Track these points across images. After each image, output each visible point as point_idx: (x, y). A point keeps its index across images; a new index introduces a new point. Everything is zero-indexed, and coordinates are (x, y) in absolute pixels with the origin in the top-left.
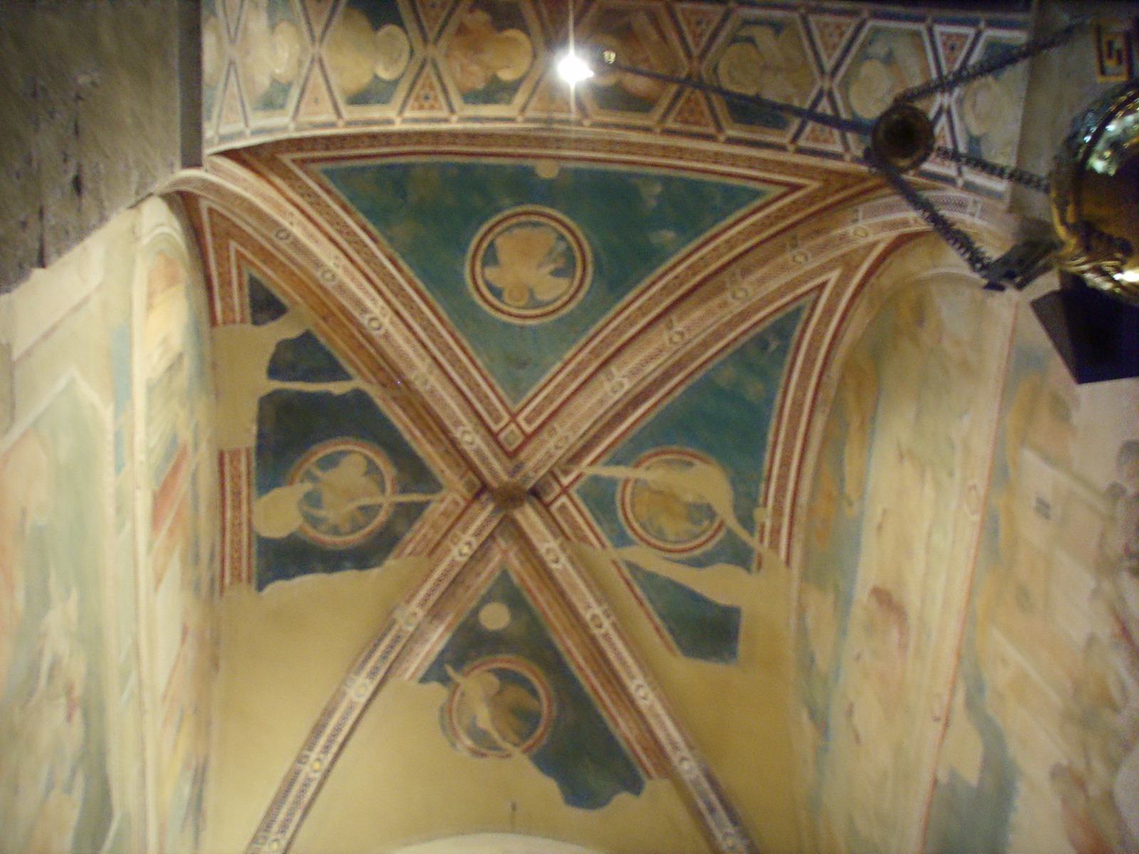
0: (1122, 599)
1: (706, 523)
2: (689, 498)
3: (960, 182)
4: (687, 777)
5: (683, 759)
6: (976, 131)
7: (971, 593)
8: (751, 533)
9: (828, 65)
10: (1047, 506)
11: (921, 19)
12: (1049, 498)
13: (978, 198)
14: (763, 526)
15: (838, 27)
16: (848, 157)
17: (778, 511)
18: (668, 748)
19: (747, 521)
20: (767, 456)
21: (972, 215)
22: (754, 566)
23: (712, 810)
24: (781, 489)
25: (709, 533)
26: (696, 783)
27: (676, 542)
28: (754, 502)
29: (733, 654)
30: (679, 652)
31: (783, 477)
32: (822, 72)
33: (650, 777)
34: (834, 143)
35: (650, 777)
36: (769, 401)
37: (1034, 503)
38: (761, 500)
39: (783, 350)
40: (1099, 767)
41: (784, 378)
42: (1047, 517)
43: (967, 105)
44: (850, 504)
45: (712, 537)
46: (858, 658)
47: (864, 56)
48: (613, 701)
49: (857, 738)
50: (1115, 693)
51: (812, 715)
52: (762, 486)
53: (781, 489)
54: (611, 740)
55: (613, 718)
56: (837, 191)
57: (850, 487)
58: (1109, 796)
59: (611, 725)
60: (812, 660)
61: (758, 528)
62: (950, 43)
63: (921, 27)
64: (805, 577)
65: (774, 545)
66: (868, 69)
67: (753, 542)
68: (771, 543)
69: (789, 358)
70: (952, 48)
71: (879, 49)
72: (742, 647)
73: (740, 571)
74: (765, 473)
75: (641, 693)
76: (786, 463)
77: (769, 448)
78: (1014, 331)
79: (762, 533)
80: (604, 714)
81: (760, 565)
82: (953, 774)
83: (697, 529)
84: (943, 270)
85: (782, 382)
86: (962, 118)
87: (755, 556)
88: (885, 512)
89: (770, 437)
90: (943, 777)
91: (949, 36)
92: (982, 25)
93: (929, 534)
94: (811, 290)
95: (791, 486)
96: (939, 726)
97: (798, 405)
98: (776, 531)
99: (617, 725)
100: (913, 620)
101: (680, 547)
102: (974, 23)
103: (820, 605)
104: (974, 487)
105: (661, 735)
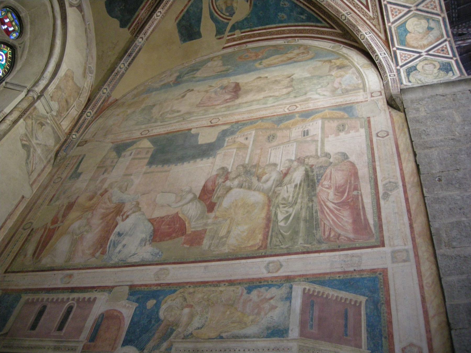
0: (295, 170)
1: (228, 14)
2: (235, 5)
3: (398, 68)
4: (136, 42)
5: (142, 38)
6: (419, 67)
7: (262, 119)
8: (230, 31)
9: (420, 7)
10: (308, 134)
11: (448, 36)
12: (311, 133)
13: (396, 76)
14: (234, 35)
15: (436, 7)
16: (390, 24)
17: (241, 38)
18: (144, 31)
19: (234, 28)
20: (260, 28)
21: (390, 76)
22: (219, 37)
23: (129, 56)
24: (250, 37)
25: (224, 16)
26: (136, 46)
27: (216, 6)
28: (241, 29)
29: (184, 41)
30: (177, 21)
31: (254, 36)
32: (417, 5)
33: (129, 29)
34: (393, 18)
35: (129, 29)
36: (281, 22)
37: (306, 129)
38: (243, 31)
39: (302, 21)
40: (236, 182)
41: (292, 24)
42: (304, 136)
43: (426, 62)
44: (260, 64)
45: (224, 18)
46: (211, 86)
47: (428, 19)
48: (150, 4)
49: (183, 97)
50: (264, 178)
51: (179, 77)
52: (248, 29)
53: (250, 37)
54: (135, 10)
55: (144, 6)
56: (372, 23)
57: (266, 62)
58: (230, 189)
59: (141, 7)
60: (198, 70)
61: (233, 33)
62: (444, 49)
63: (445, 37)
64: (223, 56)
65: (228, 41)
66: (424, 22)
67: (227, 33)
68: (229, 39)
69: (300, 24)
70: (443, 50)
71: (432, 24)
72: (189, 43)
73: (215, 33)
74: (253, 29)
75: (159, 14)
76: (260, 35)
77: (263, 27)
78: (357, 103)
79: (231, 35)
80: (144, 4)
81: (220, 38)
82: (197, 135)
83: (224, 12)
84: (361, 70)
85: (290, 24)
86: (420, 61)
87: (222, 36)
88: (267, 77)
89: (267, 26)
90: (193, 132)
91: (446, 48)
92: (455, 59)
93: (271, 96)
94: (328, 23)
95: (252, 39)
96: (210, 124)
97: (283, 32)
98: (234, 40)
99: (142, 9)
100: (238, 101)
101: (215, 7)
102: (454, 55)
103: (217, 65)
104: (297, 107)
105: (147, 27)
